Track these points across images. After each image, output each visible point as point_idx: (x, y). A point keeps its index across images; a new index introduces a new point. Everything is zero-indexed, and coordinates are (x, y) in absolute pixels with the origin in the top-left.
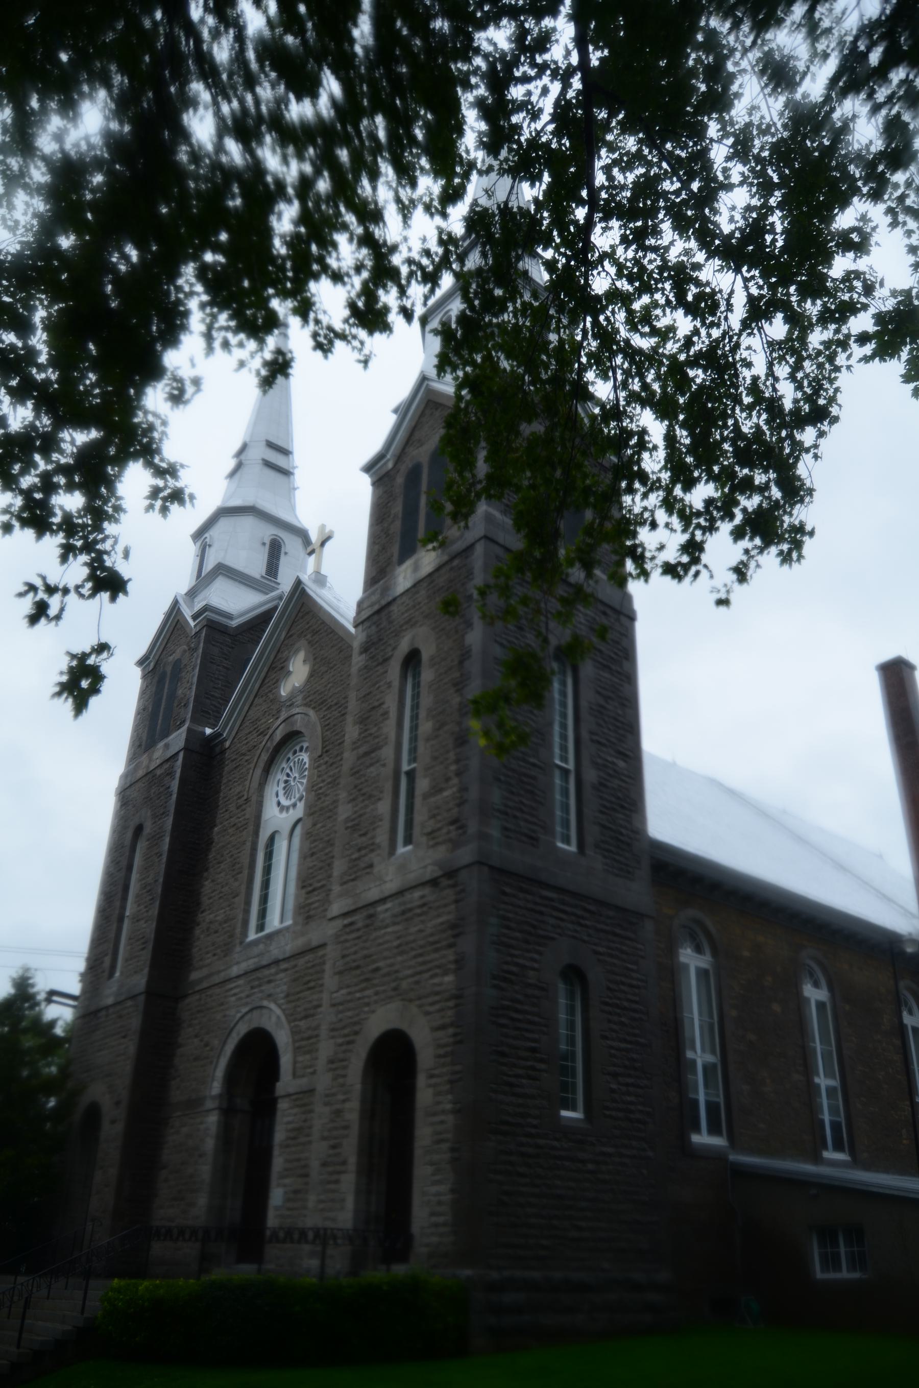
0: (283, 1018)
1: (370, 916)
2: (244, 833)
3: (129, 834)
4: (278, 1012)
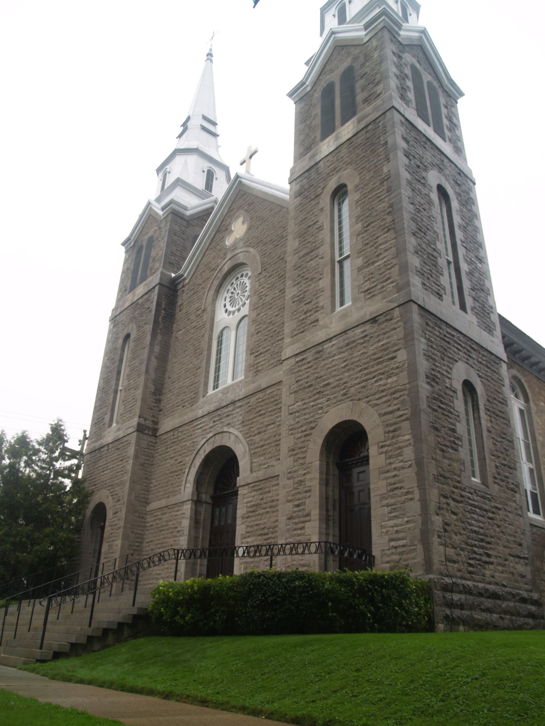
0: (240, 436)
2: (203, 330)
3: (121, 341)
4: (236, 433)
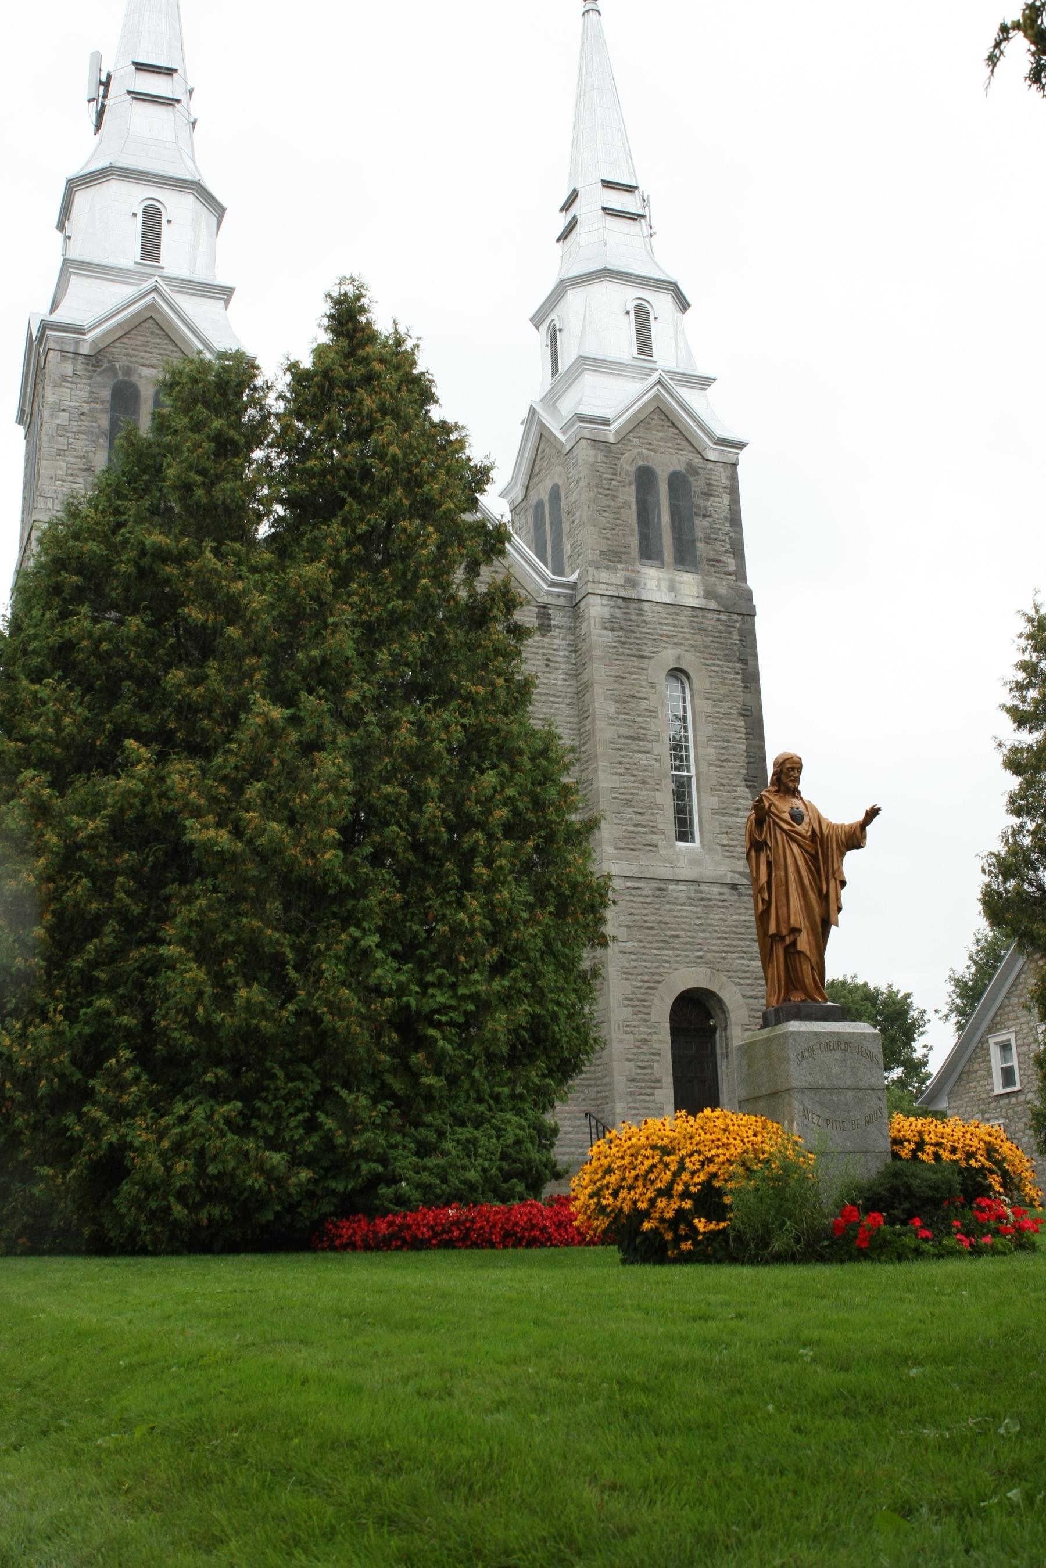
1: (660, 889)
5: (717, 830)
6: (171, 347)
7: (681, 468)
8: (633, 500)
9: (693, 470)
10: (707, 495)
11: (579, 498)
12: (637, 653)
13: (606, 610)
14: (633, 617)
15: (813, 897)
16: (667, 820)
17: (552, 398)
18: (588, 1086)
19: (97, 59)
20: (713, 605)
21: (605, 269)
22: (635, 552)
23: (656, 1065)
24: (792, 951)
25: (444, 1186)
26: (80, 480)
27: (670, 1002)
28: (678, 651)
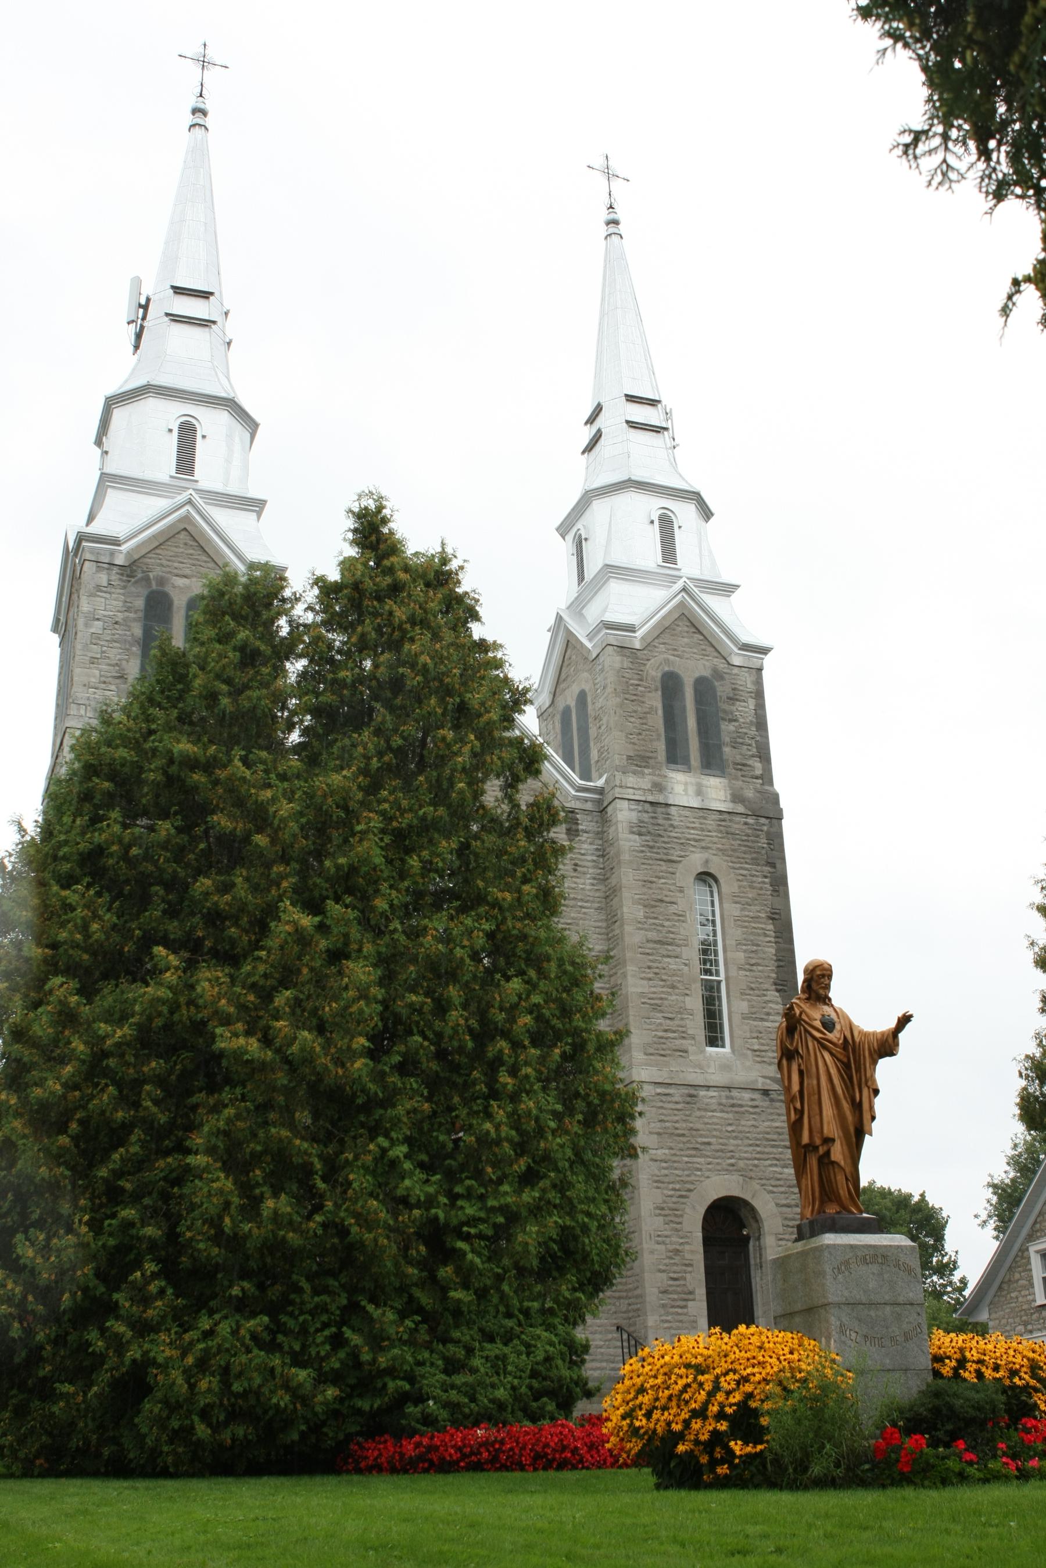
1: (691, 1096)
5: (748, 1035)
6: (204, 558)
7: (707, 673)
8: (659, 705)
9: (718, 675)
10: (732, 699)
11: (606, 703)
12: (665, 857)
13: (634, 814)
14: (660, 821)
15: (846, 1106)
16: (697, 1025)
17: (578, 606)
18: (620, 1298)
19: (137, 283)
20: (740, 809)
21: (629, 480)
22: (662, 756)
23: (688, 1276)
24: (825, 1162)
25: (473, 1405)
26: (113, 687)
27: (702, 1211)
28: (706, 855)
